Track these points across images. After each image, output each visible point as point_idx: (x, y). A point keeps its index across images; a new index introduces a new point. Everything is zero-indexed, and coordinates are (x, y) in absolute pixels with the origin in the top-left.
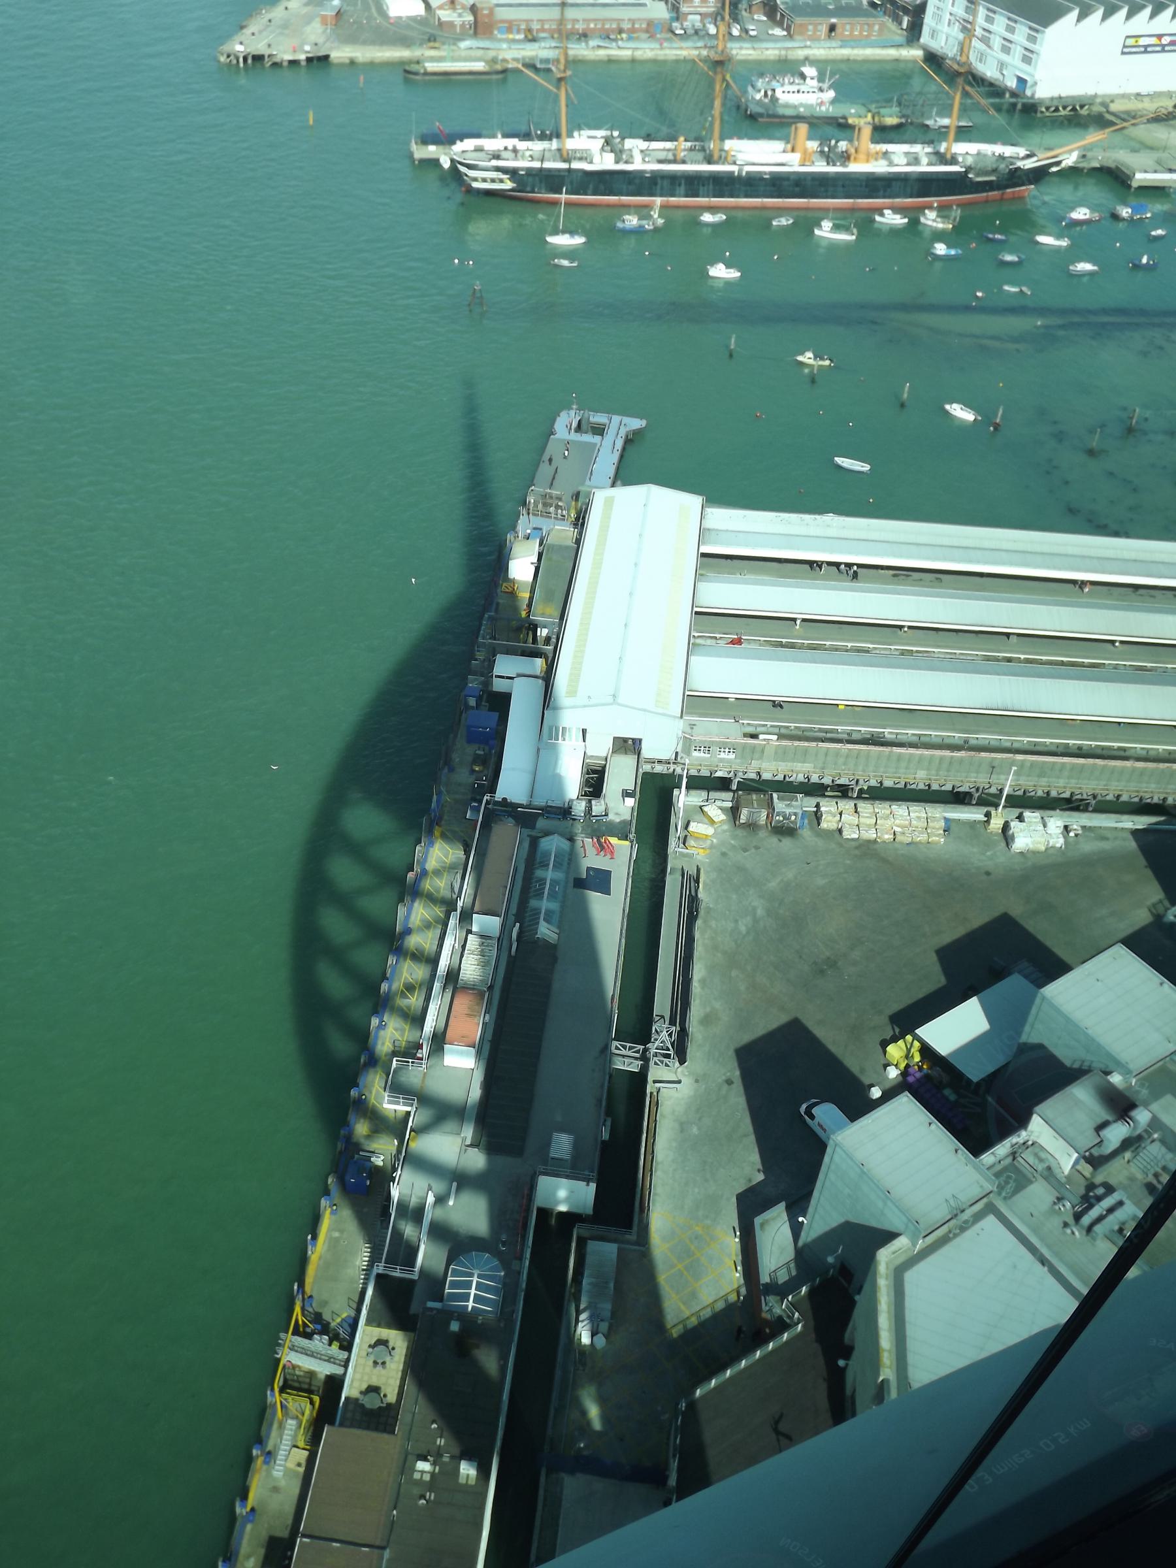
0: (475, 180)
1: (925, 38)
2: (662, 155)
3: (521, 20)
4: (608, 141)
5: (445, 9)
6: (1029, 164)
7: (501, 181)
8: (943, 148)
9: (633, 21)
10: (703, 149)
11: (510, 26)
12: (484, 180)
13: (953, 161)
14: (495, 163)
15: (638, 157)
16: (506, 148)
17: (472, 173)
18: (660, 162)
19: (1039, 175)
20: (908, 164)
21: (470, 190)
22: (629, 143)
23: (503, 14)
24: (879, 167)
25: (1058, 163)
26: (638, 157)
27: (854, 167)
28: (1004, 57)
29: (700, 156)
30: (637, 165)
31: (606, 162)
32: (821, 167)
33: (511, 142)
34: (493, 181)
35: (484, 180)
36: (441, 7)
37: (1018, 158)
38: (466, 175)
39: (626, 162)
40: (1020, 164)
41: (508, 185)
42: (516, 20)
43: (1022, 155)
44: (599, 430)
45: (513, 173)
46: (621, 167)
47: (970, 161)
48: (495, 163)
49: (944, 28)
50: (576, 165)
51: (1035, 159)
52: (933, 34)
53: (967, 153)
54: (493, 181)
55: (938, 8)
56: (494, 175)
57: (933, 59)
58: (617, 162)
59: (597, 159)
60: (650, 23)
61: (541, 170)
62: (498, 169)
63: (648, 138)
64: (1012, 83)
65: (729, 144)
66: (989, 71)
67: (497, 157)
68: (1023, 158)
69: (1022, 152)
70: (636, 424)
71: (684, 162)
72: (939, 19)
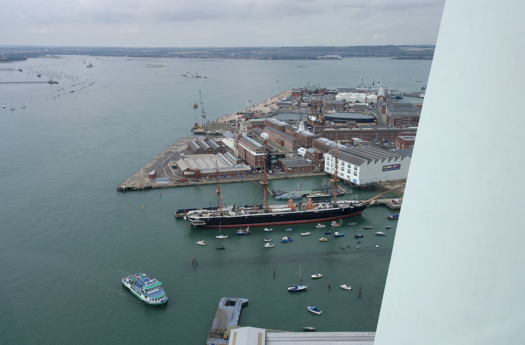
0: (194, 223)
1: (326, 170)
2: (250, 211)
3: (208, 173)
5: (186, 171)
6: (360, 205)
7: (202, 223)
8: (333, 202)
9: (241, 171)
10: (262, 208)
11: (205, 175)
12: (197, 223)
13: (336, 206)
16: (204, 212)
17: (194, 221)
18: (250, 213)
21: (192, 226)
23: (203, 172)
24: (316, 210)
25: (369, 204)
26: (243, 212)
28: (349, 174)
29: (262, 211)
31: (233, 214)
32: (297, 211)
33: (205, 211)
34: (200, 223)
35: (197, 223)
36: (185, 171)
37: (356, 203)
38: (191, 221)
39: (239, 215)
40: (357, 205)
41: (205, 223)
42: (207, 173)
43: (357, 203)
44: (233, 304)
45: (205, 220)
46: (238, 216)
47: (342, 206)
48: (200, 217)
49: (330, 167)
50: (225, 216)
51: (361, 203)
52: (328, 169)
53: (341, 203)
54: (200, 223)
55: (328, 162)
57: (329, 176)
58: (237, 215)
60: (246, 171)
61: (214, 218)
62: (200, 219)
63: (246, 206)
64: (352, 181)
65: (270, 206)
66: (345, 178)
67: (201, 216)
68: (358, 204)
69: (358, 202)
70: (245, 300)
71: (257, 213)
72: (328, 165)
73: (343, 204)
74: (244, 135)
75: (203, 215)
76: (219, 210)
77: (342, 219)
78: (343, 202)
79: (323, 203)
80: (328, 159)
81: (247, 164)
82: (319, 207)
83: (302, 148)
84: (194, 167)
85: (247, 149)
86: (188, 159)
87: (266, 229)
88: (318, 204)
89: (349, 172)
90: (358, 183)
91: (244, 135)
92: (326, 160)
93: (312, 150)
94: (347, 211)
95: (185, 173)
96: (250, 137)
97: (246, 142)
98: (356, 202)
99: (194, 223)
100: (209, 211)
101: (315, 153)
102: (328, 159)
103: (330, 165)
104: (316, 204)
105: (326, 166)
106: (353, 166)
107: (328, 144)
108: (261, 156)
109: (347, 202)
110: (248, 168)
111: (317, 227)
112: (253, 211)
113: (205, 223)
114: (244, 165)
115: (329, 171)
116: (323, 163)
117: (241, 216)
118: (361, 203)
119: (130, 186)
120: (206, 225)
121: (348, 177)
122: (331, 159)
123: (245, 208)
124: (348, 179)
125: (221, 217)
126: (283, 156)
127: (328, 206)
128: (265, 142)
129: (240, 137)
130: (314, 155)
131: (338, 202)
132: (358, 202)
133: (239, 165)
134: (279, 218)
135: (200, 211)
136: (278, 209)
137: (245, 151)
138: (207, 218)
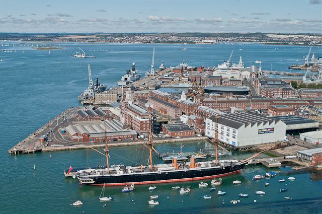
0: (83, 181)
1: (206, 134)
2: (137, 170)
4: (121, 168)
6: (239, 164)
12: (86, 181)
14: (88, 176)
15: (130, 171)
19: (242, 166)
20: (206, 167)
22: (127, 168)
23: (91, 136)
24: (198, 168)
27: (191, 169)
30: (130, 173)
32: (181, 170)
33: (93, 170)
34: (88, 181)
35: (86, 181)
41: (93, 182)
45: (94, 179)
46: (125, 174)
47: (222, 165)
48: (88, 176)
52: (208, 133)
54: (88, 181)
56: (89, 179)
59: (118, 173)
62: (90, 177)
64: (231, 143)
65: (155, 166)
66: (224, 141)
67: (90, 174)
69: (237, 161)
71: (143, 172)
72: (209, 129)
73: (223, 163)
74: (130, 103)
75: (91, 173)
76: (107, 169)
77: (221, 177)
78: (223, 161)
79: (205, 163)
80: (209, 124)
81: (132, 129)
82: (202, 166)
83: (184, 115)
84: (82, 132)
85: (133, 116)
86: (77, 126)
87: (150, 188)
88: (201, 163)
89: (228, 135)
90: (236, 145)
91: (130, 103)
92: (207, 125)
93: (193, 117)
94: (227, 169)
95: (75, 137)
96: (135, 105)
97: (131, 109)
98: (236, 161)
99: (83, 181)
100: (96, 171)
101: (196, 119)
102: (209, 124)
103: (211, 129)
104: (199, 163)
105: (207, 130)
106: (231, 129)
107: (208, 111)
108: (146, 121)
109: (228, 161)
110: (134, 132)
111: (200, 185)
112: (139, 170)
113: (93, 182)
114: (130, 130)
115: (210, 136)
116: (204, 127)
117: (128, 174)
118: (240, 162)
119: (21, 149)
120: (94, 183)
121: (228, 140)
122: (211, 124)
123: (132, 168)
124: (227, 142)
125: (109, 175)
126: (166, 123)
127: (210, 165)
128: (150, 109)
129: (126, 106)
130: (195, 121)
131: (220, 161)
132: (237, 161)
133: (126, 130)
134: (163, 176)
135: (89, 171)
136: (162, 168)
137: (131, 117)
138: (96, 177)
